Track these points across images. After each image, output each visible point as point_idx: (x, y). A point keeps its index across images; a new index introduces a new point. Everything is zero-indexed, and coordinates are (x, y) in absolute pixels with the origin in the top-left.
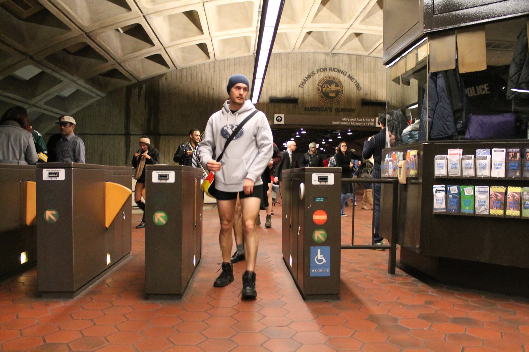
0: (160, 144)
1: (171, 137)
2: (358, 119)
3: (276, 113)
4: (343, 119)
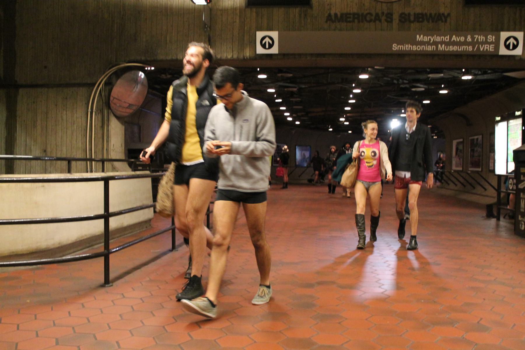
0: (18, 108)
1: (39, 90)
2: (454, 38)
3: (261, 30)
4: (419, 38)
